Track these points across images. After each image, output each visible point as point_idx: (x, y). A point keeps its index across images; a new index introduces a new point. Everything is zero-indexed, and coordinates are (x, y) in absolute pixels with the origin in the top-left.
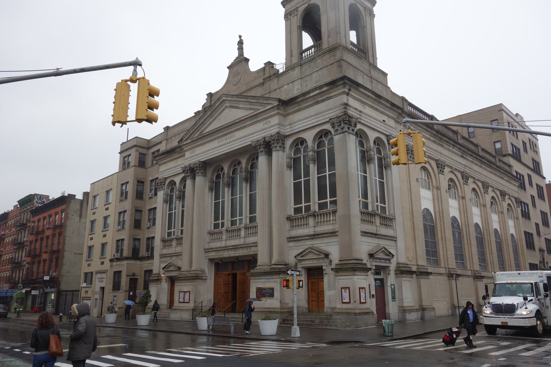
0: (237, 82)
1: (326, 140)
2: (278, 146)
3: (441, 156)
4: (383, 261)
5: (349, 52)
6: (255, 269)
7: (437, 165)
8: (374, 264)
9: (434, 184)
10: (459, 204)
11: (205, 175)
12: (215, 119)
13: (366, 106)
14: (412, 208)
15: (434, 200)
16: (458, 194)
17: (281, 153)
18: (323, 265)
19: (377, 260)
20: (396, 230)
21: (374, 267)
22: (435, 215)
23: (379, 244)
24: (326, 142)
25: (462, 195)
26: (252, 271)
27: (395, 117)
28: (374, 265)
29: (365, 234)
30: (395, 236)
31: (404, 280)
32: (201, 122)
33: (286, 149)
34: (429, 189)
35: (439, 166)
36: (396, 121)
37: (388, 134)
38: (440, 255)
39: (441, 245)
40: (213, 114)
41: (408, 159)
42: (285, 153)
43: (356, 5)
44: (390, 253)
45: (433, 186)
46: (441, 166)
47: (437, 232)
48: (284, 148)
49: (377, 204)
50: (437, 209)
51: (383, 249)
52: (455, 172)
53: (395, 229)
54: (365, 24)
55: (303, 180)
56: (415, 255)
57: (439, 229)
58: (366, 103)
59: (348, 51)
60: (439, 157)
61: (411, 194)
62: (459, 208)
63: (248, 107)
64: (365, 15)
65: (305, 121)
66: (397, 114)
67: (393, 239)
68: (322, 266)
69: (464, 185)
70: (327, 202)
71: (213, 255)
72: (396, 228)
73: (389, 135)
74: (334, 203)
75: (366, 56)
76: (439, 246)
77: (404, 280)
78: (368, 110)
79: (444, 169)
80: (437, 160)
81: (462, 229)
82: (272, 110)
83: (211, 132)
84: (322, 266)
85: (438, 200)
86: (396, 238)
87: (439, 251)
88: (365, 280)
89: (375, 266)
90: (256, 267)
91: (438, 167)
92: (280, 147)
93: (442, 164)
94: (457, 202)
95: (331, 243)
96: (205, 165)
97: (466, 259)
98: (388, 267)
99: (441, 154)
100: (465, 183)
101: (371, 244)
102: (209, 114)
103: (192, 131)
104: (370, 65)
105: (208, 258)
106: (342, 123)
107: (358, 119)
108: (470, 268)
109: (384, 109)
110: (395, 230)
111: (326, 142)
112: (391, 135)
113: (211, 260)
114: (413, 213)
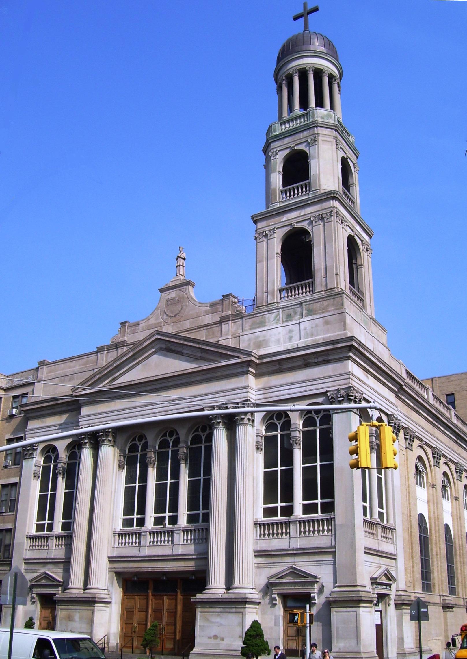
0: (174, 314)
1: (318, 417)
2: (246, 418)
3: (437, 442)
4: (385, 587)
5: (352, 302)
6: (203, 592)
7: (433, 454)
8: (377, 591)
9: (430, 481)
10: (452, 508)
11: (114, 444)
12: (138, 364)
13: (369, 375)
14: (410, 514)
15: (428, 502)
16: (451, 494)
17: (250, 427)
18: (311, 592)
19: (383, 587)
20: (396, 545)
21: (377, 596)
22: (430, 523)
23: (380, 564)
24: (318, 421)
25: (455, 495)
26: (199, 596)
27: (396, 390)
28: (376, 592)
29: (369, 551)
30: (396, 553)
31: (405, 613)
32: (115, 365)
33: (255, 422)
34: (424, 487)
35: (435, 456)
36: (397, 396)
37: (390, 413)
38: (434, 578)
39: (435, 563)
40: (136, 356)
41: (406, 446)
42: (255, 428)
43: (354, 236)
44: (392, 577)
45: (427, 482)
46: (437, 455)
47: (432, 545)
48: (253, 421)
49: (381, 510)
50: (432, 514)
51: (386, 572)
52: (450, 463)
53: (395, 543)
54: (363, 263)
55: (279, 468)
56: (412, 578)
57: (434, 542)
58: (369, 371)
59: (350, 300)
60: (435, 443)
61: (409, 496)
62: (452, 513)
63: (199, 355)
64: (363, 250)
65: (288, 387)
66: (399, 387)
67: (392, 557)
68: (310, 593)
69: (457, 482)
70: (317, 504)
71: (122, 567)
72: (396, 542)
73: (391, 415)
74: (329, 508)
75: (363, 305)
76: (433, 566)
77: (405, 613)
78: (371, 381)
79: (440, 459)
80: (434, 448)
81: (455, 542)
82: (238, 366)
83: (133, 383)
84: (310, 593)
85: (433, 502)
86: (396, 555)
87: (433, 572)
88: (369, 613)
89: (378, 594)
90: (205, 590)
91: (434, 457)
92: (249, 419)
93: (439, 453)
94: (450, 504)
95: (324, 562)
96: (117, 430)
97: (458, 582)
98: (388, 595)
99: (437, 439)
100: (458, 478)
101: (372, 564)
102: (130, 355)
103: (98, 377)
104: (371, 318)
105: (115, 570)
106: (346, 398)
107: (363, 394)
108: (463, 595)
109: (386, 379)
110: (395, 545)
111: (318, 421)
112: (393, 415)
113: (118, 574)
114: (411, 521)
